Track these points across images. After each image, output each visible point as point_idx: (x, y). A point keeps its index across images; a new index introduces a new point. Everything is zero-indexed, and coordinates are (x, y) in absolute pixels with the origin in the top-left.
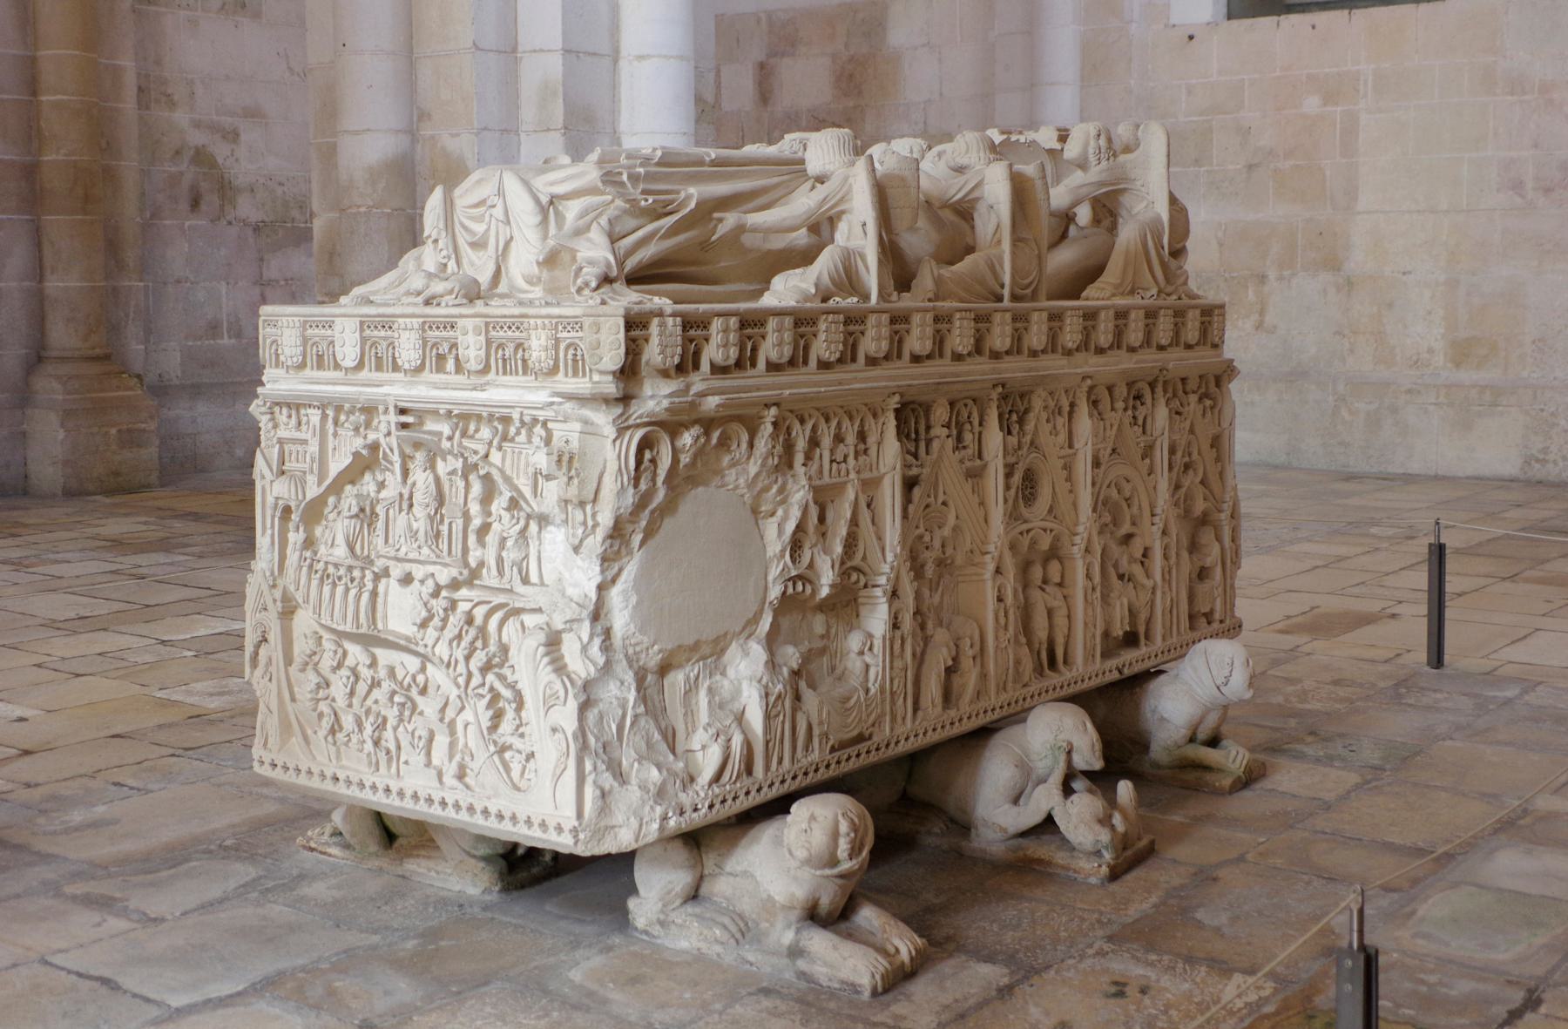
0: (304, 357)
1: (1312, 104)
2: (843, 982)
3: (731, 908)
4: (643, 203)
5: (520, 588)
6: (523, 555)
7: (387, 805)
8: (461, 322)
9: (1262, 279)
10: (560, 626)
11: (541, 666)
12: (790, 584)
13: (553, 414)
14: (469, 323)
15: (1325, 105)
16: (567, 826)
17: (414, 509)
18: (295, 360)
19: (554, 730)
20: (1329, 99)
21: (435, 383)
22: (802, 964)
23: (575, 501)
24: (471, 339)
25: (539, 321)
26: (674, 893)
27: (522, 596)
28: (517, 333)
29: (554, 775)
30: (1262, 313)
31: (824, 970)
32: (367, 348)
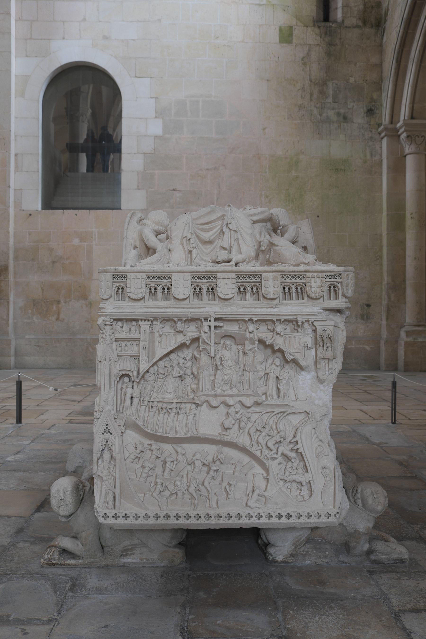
1: (76, 241)
2: (396, 560)
7: (199, 524)
8: (264, 275)
9: (59, 302)
11: (313, 439)
13: (322, 318)
14: (270, 276)
15: (81, 242)
19: (324, 468)
20: (82, 240)
21: (243, 305)
22: (373, 557)
24: (271, 283)
25: (315, 274)
26: (301, 540)
27: (294, 407)
28: (298, 280)
30: (59, 314)
31: (385, 557)
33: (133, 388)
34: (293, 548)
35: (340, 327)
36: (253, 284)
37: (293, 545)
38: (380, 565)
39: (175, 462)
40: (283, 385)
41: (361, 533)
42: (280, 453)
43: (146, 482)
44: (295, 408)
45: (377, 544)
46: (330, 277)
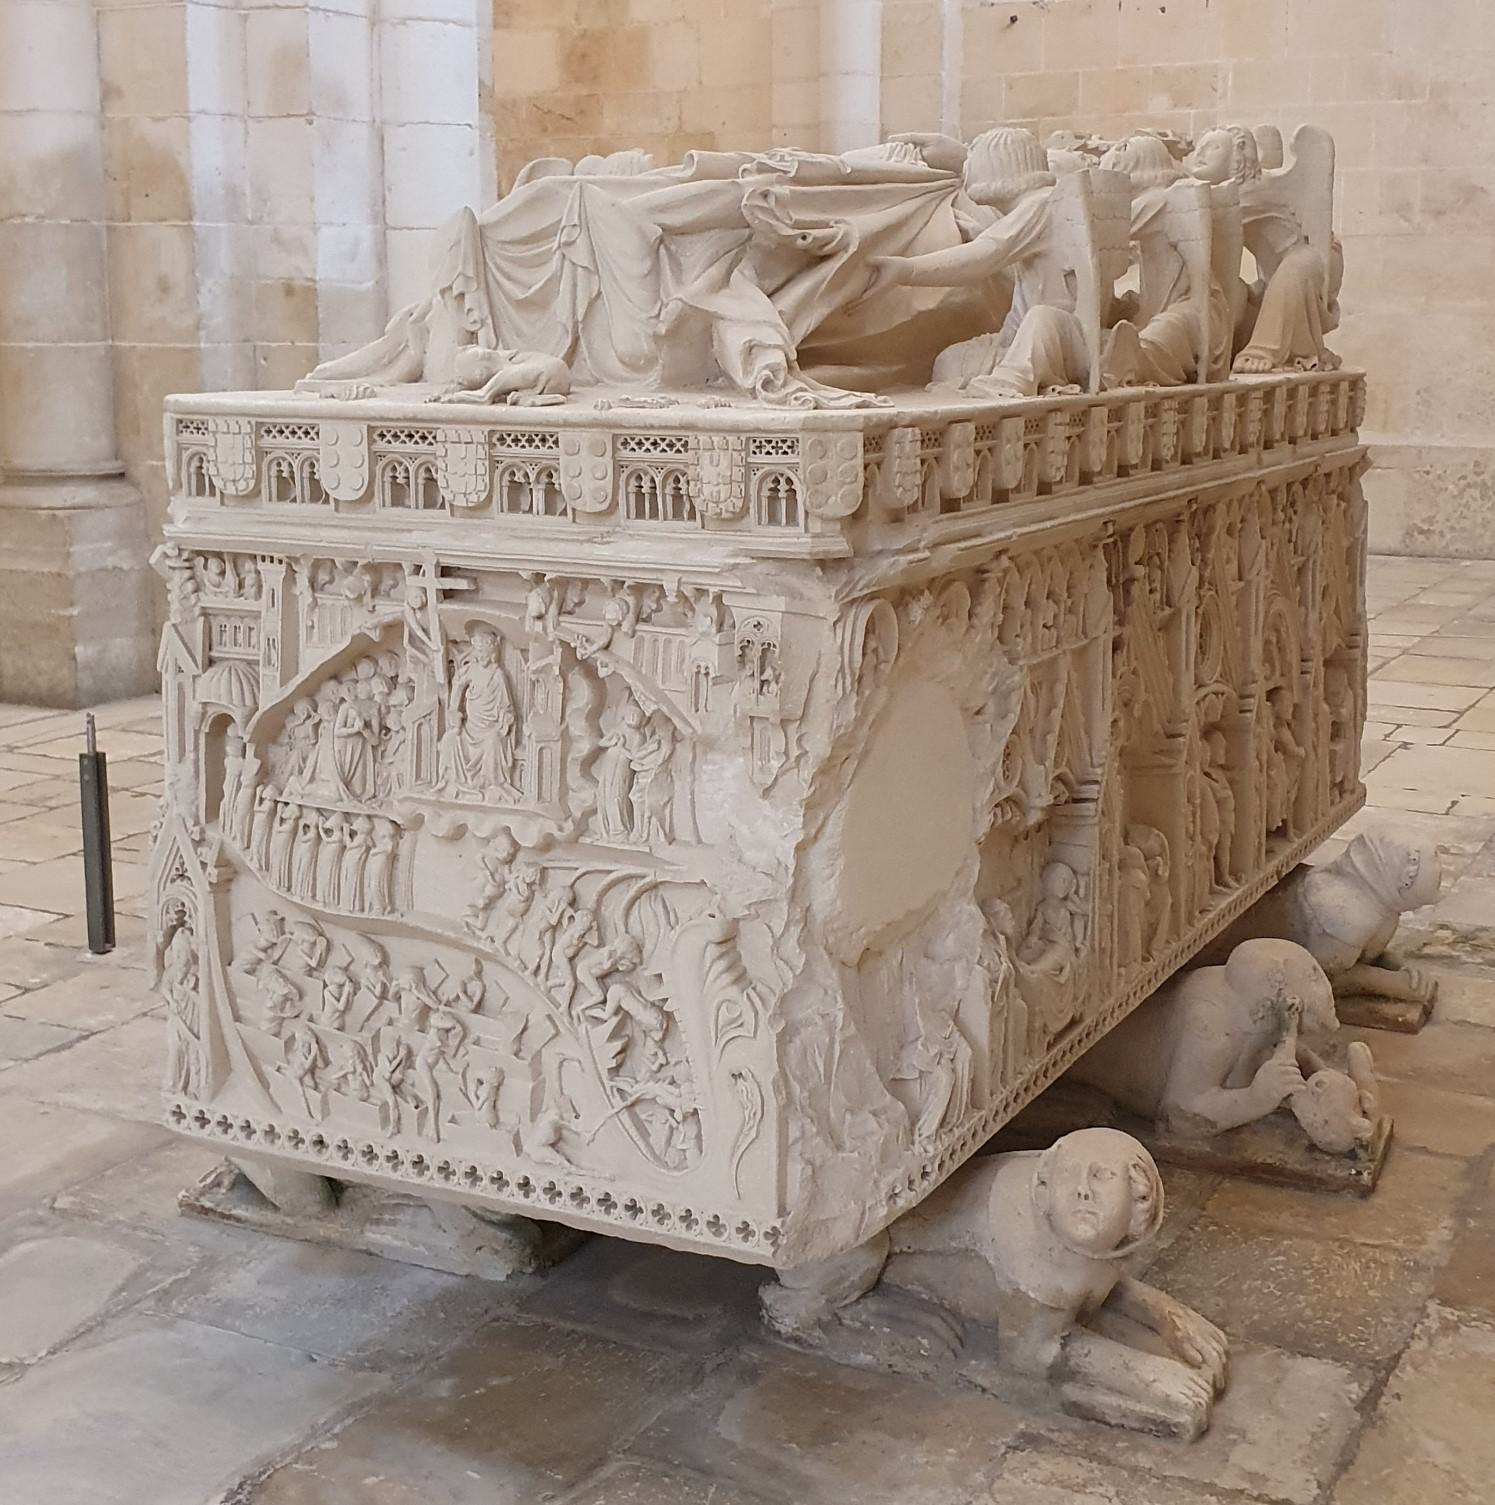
0: (258, 482)
3: (936, 1300)
4: (800, 241)
5: (665, 852)
6: (666, 799)
10: (741, 913)
11: (711, 977)
12: (998, 811)
13: (740, 584)
14: (584, 437)
16: (759, 1229)
17: (468, 724)
18: (242, 485)
19: (737, 1076)
22: (1072, 1392)
23: (775, 719)
24: (585, 460)
26: (847, 1284)
27: (673, 864)
29: (735, 1147)
32: (378, 471)
33: (244, 757)
34: (823, 1302)
35: (821, 615)
36: (544, 462)
37: (823, 1293)
38: (1093, 1423)
39: (348, 988)
40: (641, 790)
41: (1033, 1305)
42: (610, 1006)
43: (276, 1035)
44: (671, 868)
45: (1089, 1352)
46: (768, 448)
